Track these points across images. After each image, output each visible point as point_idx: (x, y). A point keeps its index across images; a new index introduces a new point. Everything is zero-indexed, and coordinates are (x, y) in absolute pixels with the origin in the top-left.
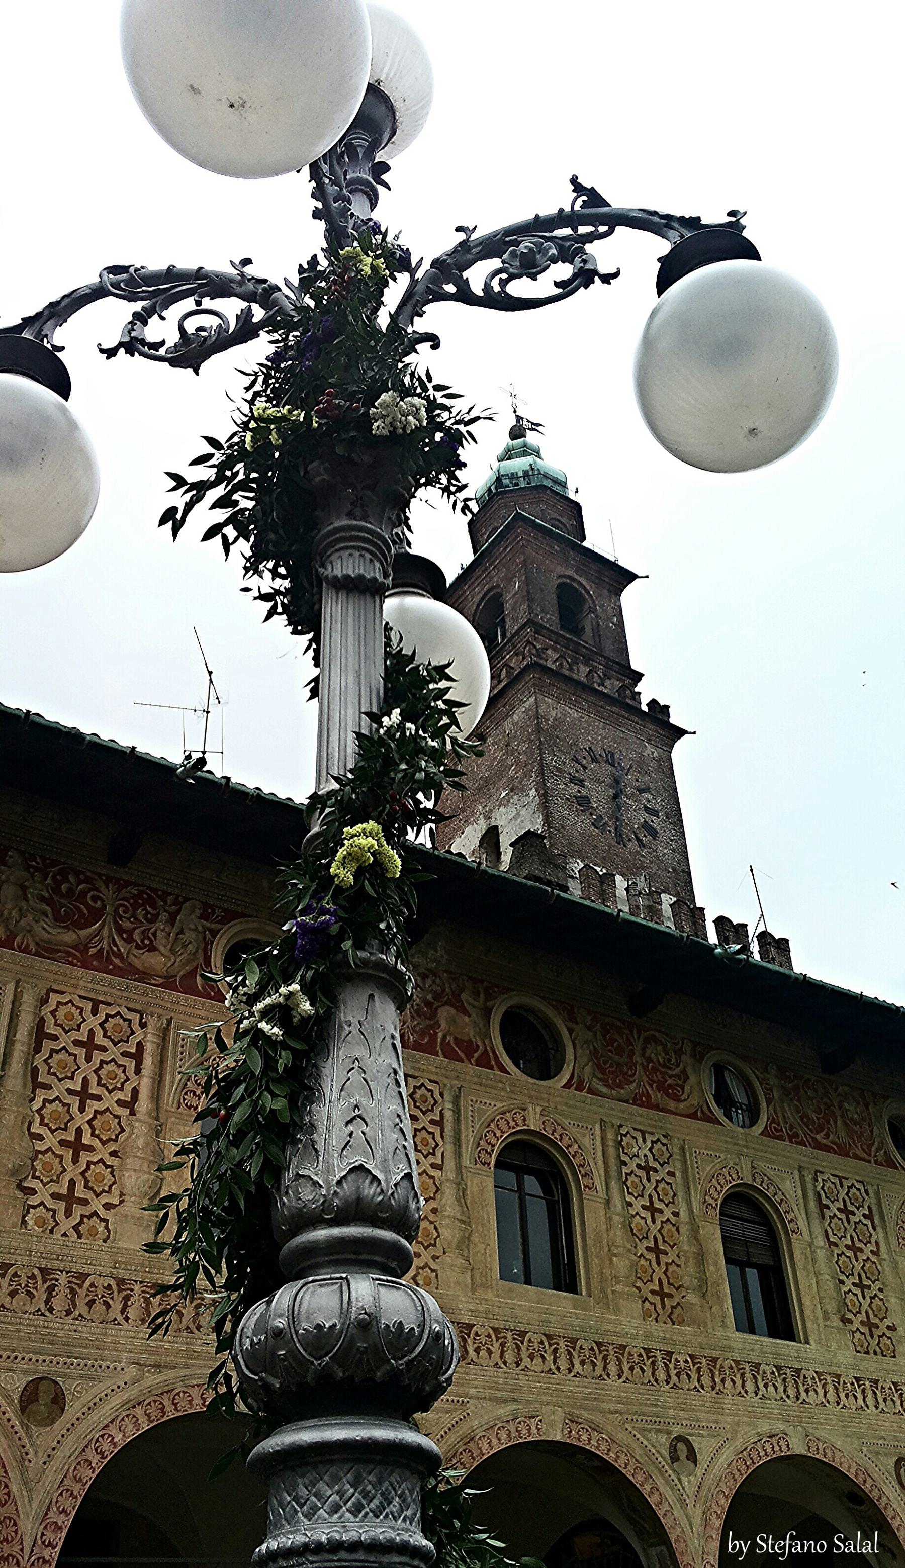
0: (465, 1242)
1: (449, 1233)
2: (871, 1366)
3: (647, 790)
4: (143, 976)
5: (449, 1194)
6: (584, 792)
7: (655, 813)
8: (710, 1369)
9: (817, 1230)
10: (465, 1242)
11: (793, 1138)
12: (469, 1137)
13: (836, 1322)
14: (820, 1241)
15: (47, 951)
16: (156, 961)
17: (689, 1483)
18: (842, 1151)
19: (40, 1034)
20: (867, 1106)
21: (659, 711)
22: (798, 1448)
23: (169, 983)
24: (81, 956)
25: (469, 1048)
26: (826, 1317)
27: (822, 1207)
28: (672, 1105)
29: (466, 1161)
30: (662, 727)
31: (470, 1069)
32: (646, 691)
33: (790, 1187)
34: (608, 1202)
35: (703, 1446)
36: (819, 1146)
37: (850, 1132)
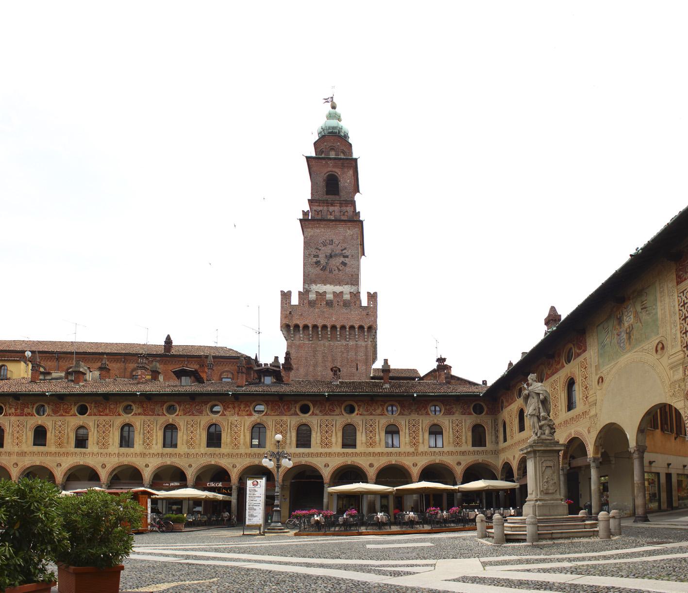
0: (26, 441)
1: (24, 441)
3: (345, 249)
5: (24, 435)
6: (318, 259)
9: (96, 430)
10: (26, 441)
11: (95, 415)
12: (28, 427)
13: (95, 445)
14: (96, 432)
18: (107, 415)
20: (117, 405)
26: (94, 444)
27: (98, 426)
28: (67, 415)
29: (27, 430)
31: (29, 417)
33: (91, 424)
34: (52, 433)
36: (100, 415)
37: (110, 411)
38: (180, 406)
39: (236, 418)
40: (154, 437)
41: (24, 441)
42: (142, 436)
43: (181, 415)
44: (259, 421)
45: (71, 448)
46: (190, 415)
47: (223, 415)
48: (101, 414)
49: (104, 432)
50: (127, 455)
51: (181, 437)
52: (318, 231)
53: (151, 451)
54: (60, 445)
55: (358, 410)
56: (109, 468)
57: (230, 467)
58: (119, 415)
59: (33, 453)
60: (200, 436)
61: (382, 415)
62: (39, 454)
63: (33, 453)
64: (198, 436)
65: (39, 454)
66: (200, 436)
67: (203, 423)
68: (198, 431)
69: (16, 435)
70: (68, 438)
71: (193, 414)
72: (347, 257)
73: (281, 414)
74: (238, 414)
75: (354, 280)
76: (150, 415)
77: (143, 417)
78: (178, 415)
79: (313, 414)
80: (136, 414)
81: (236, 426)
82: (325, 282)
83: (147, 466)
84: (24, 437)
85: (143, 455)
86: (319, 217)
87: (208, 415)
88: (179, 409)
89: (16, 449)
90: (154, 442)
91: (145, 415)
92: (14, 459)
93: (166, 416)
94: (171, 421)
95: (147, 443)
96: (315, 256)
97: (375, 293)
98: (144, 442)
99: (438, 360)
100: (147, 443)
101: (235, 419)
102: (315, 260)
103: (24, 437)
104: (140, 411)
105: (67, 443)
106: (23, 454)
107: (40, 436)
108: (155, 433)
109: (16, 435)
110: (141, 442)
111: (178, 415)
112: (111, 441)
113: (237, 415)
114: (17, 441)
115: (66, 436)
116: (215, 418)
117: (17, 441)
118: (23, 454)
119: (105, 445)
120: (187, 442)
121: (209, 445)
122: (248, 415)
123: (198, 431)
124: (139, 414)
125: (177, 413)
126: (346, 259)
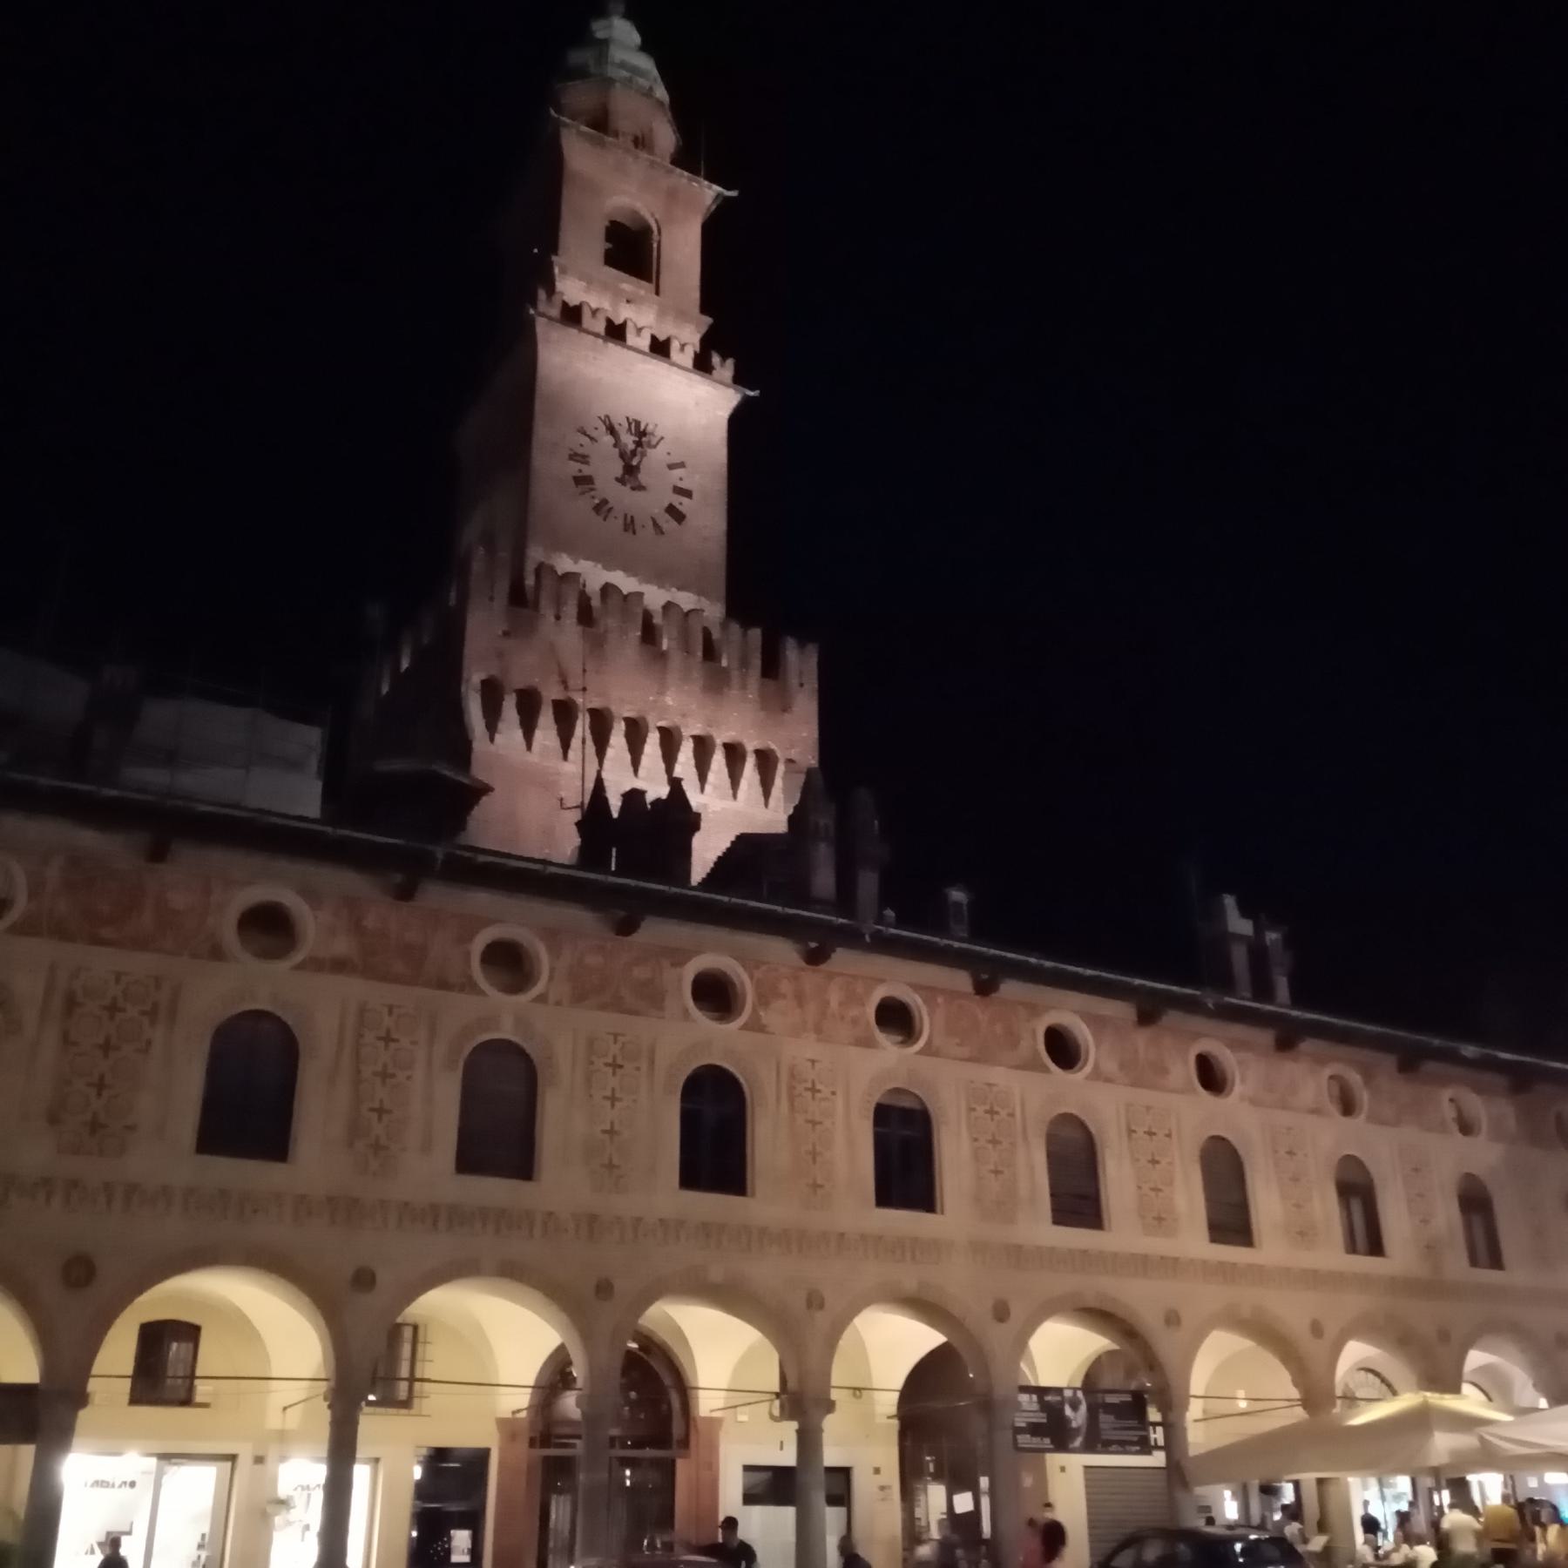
11: (61, 933)
18: (141, 944)
27: (71, 1003)
38: (555, 951)
43: (558, 1003)
46: (603, 1007)
47: (756, 1026)
48: (106, 932)
49: (106, 1047)
55: (1243, 1081)
61: (1316, 1111)
71: (617, 1006)
72: (687, 493)
73: (981, 1057)
74: (818, 1030)
77: (355, 988)
79: (1097, 1075)
80: (316, 965)
81: (814, 1090)
82: (608, 559)
87: (686, 1014)
88: (552, 970)
93: (482, 993)
94: (506, 1032)
96: (574, 457)
101: (809, 1055)
102: (574, 468)
111: (542, 999)
113: (813, 1036)
121: (691, 1177)
124: (340, 966)
126: (685, 500)
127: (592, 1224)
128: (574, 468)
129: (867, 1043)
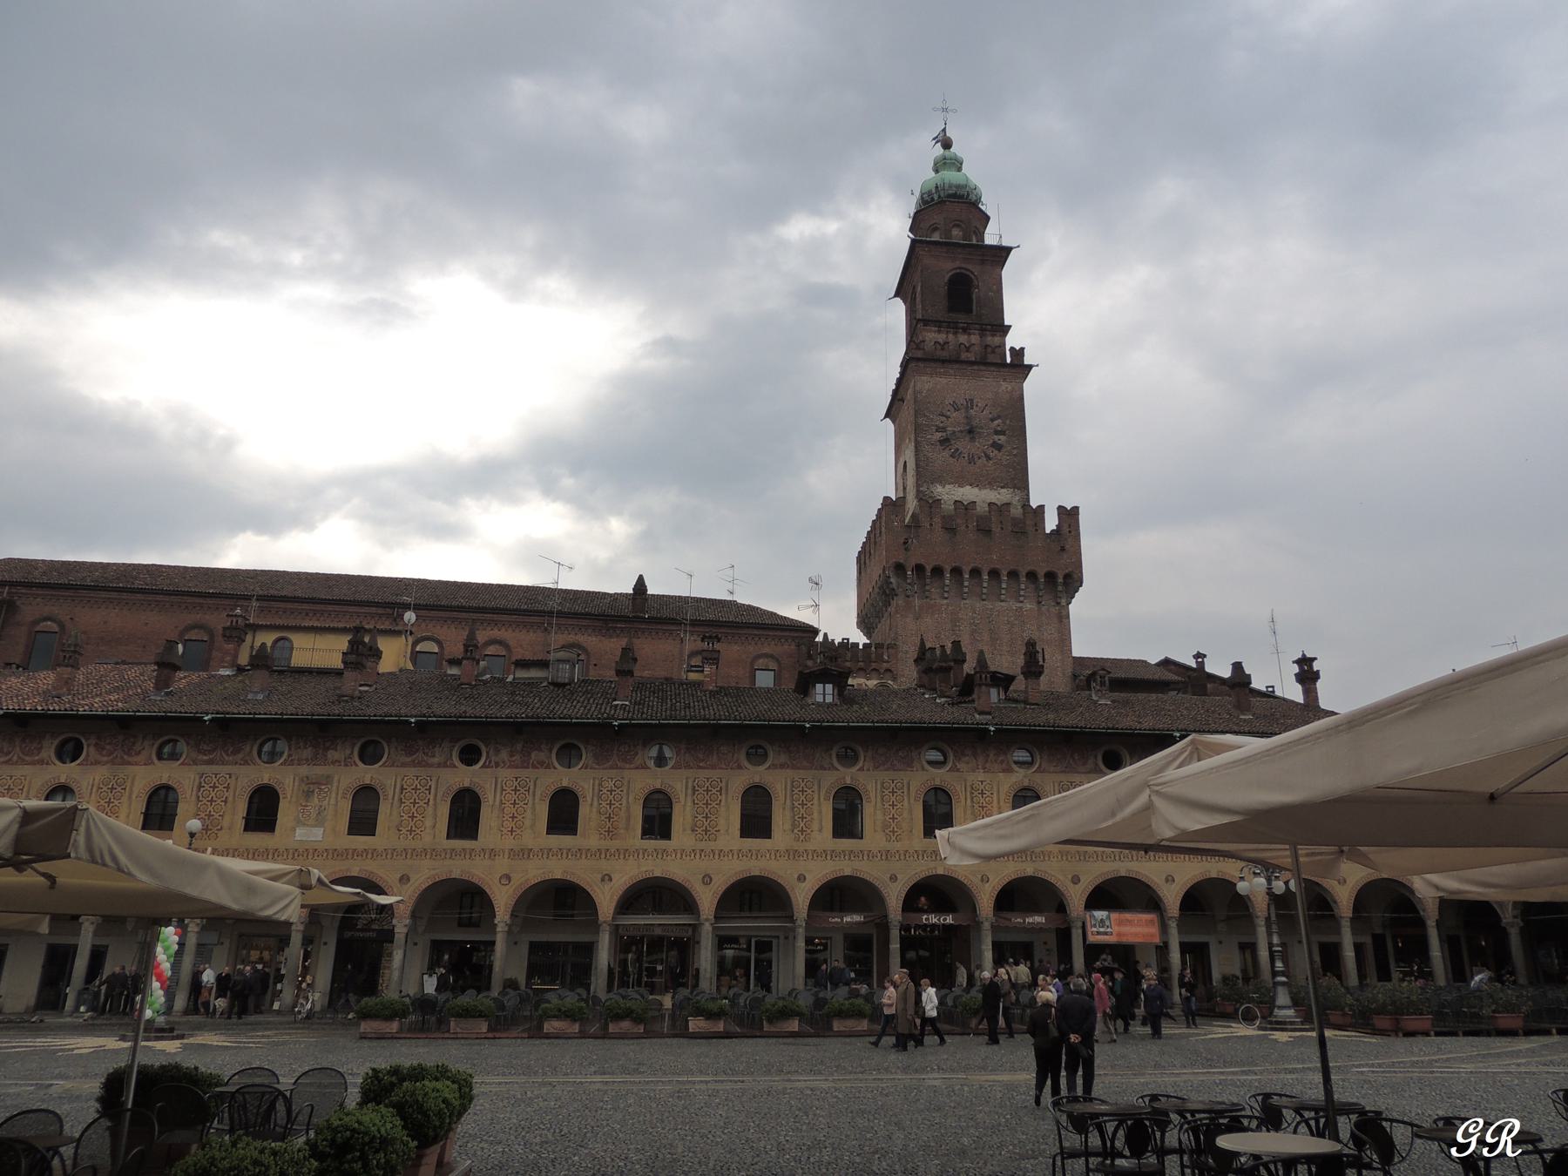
0: (533, 826)
1: (528, 822)
2: (702, 845)
4: (431, 766)
5: (529, 812)
7: (1002, 433)
8: (625, 853)
10: (533, 826)
12: (538, 793)
14: (689, 803)
15: (403, 765)
16: (436, 760)
17: (607, 887)
18: (713, 767)
19: (402, 789)
21: (1018, 353)
22: (657, 874)
23: (439, 765)
24: (413, 764)
25: (541, 764)
30: (1019, 367)
31: (542, 771)
32: (1012, 341)
35: (615, 877)
39: (981, 775)
40: (816, 815)
41: (528, 822)
42: (788, 813)
44: (1026, 783)
45: (635, 839)
50: (758, 854)
51: (872, 815)
52: (944, 381)
53: (810, 846)
54: (611, 833)
56: (721, 883)
57: (976, 880)
58: (740, 767)
59: (548, 852)
60: (910, 812)
62: (561, 852)
63: (548, 852)
64: (905, 815)
65: (561, 852)
66: (910, 812)
67: (915, 785)
68: (906, 803)
69: (509, 810)
70: (628, 819)
75: (1018, 476)
76: (805, 768)
77: (790, 772)
78: (862, 769)
80: (773, 766)
82: (960, 481)
83: (801, 878)
84: (529, 814)
85: (793, 854)
86: (945, 354)
89: (509, 842)
90: (815, 826)
91: (794, 767)
92: (502, 865)
95: (801, 829)
97: (1076, 509)
98: (794, 826)
99: (1298, 662)
100: (801, 829)
103: (529, 814)
104: (783, 758)
105: (627, 829)
106: (524, 853)
107: (564, 813)
108: (815, 808)
109: (509, 810)
110: (788, 826)
112: (722, 823)
114: (509, 824)
115: (623, 814)
116: (940, 776)
117: (509, 824)
118: (524, 853)
119: (709, 833)
120: (885, 826)
122: (1004, 771)
123: (906, 803)
124: (782, 766)
125: (860, 764)
127: (887, 855)
128: (939, 435)
129: (1008, 770)
